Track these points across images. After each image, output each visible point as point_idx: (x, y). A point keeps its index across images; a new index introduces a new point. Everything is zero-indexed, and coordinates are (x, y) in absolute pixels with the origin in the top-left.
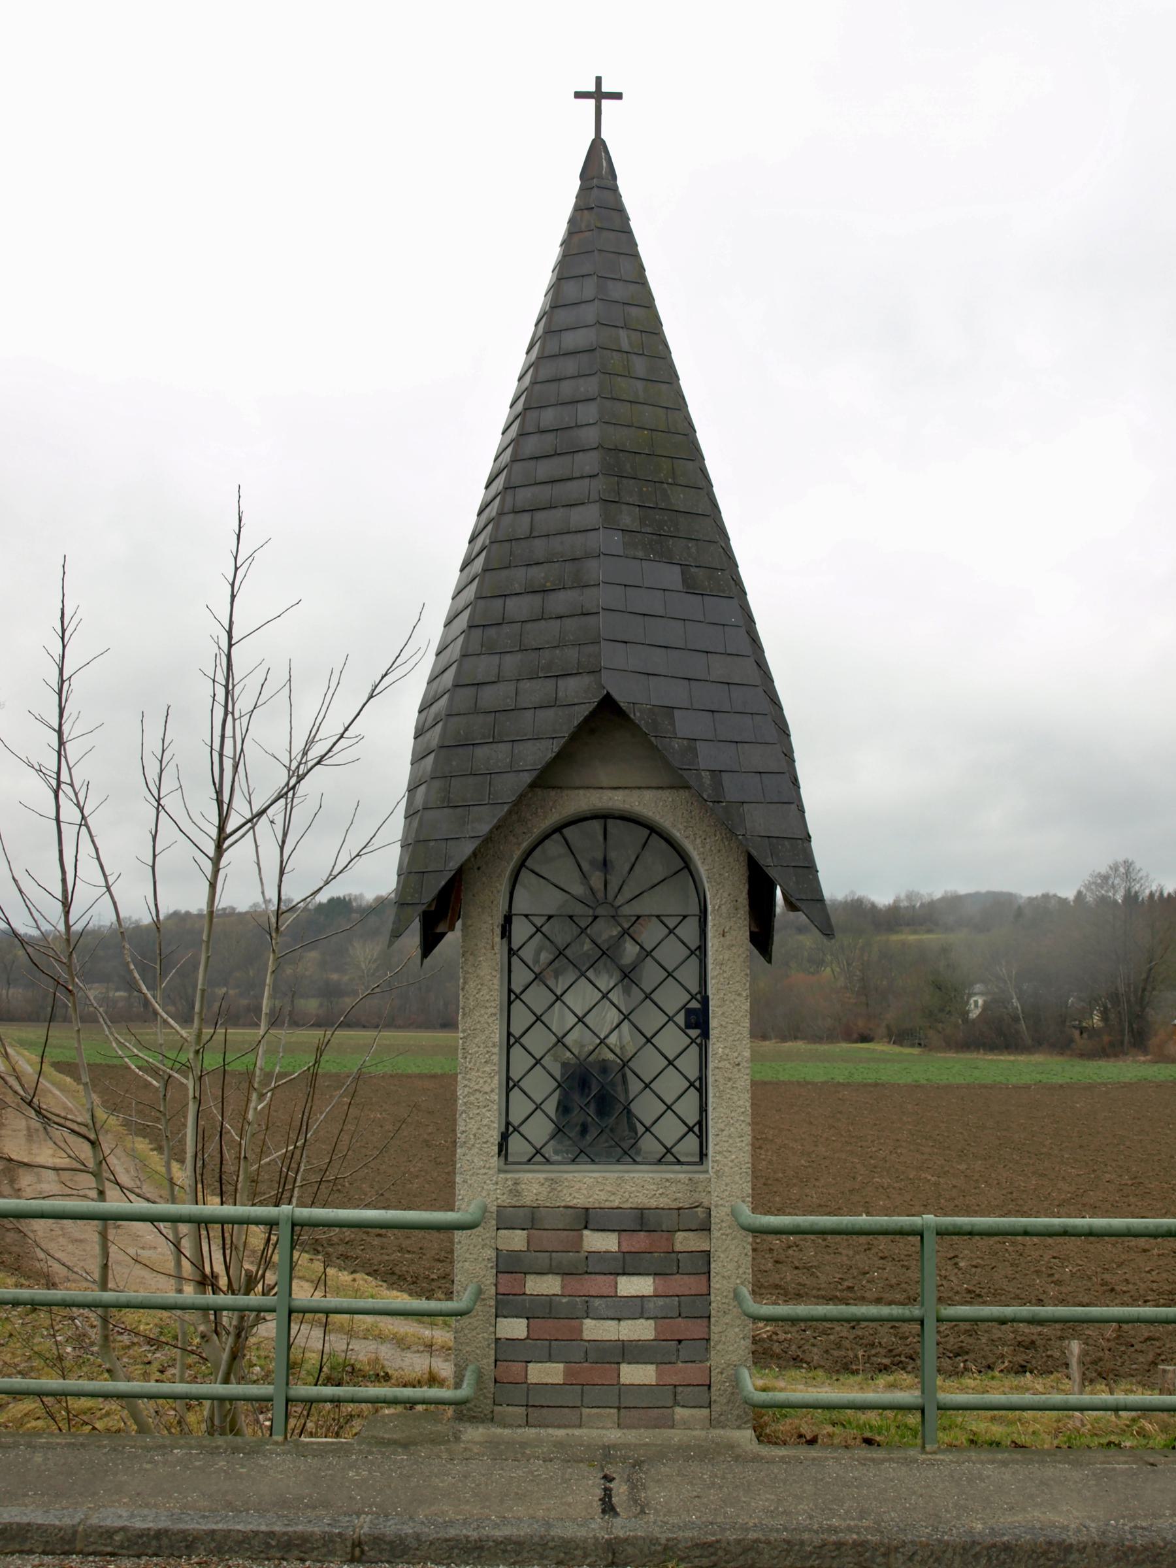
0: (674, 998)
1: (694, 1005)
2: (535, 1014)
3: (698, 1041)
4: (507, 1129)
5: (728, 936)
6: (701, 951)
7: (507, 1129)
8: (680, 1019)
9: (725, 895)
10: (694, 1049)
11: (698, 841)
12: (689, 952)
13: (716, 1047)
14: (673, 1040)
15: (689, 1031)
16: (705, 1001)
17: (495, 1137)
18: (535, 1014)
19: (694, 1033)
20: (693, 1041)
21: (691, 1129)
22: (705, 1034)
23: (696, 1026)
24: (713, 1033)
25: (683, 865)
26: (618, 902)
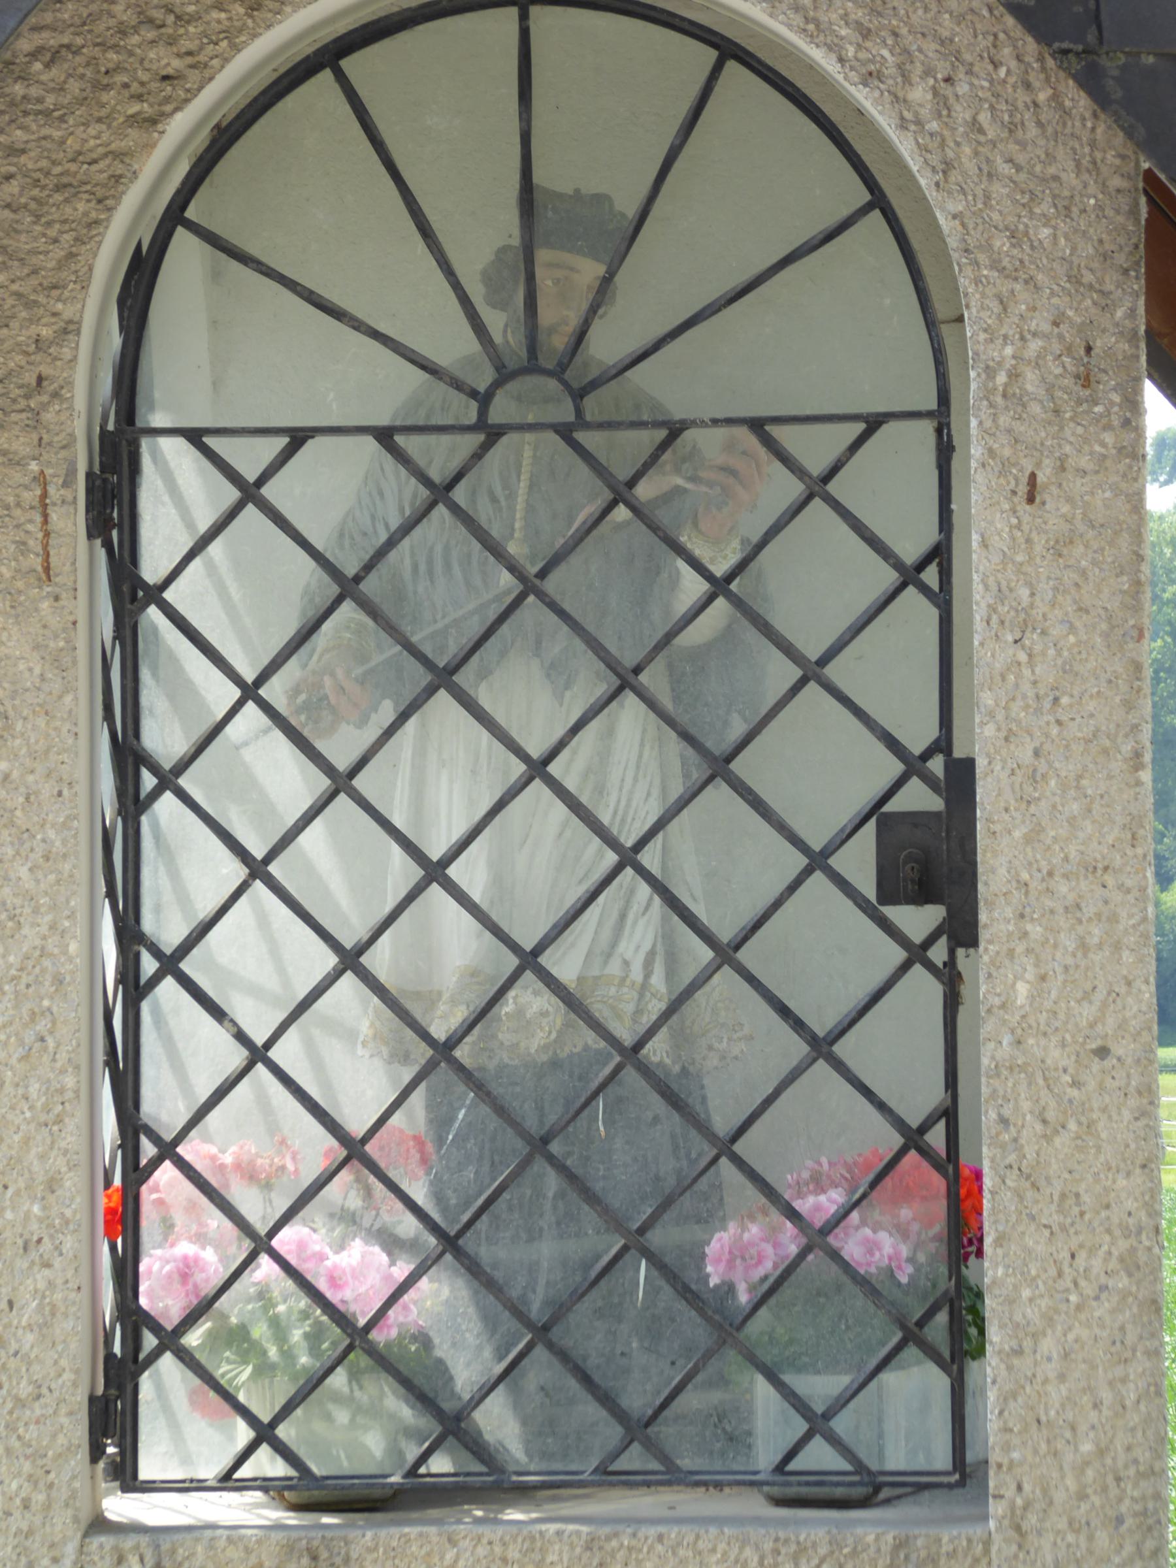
0: (828, 772)
1: (919, 798)
2: (839, 1066)
3: (938, 953)
4: (133, 1341)
5: (1054, 504)
6: (932, 572)
7: (133, 1341)
8: (859, 861)
9: (1040, 322)
10: (922, 988)
11: (919, 94)
12: (891, 577)
13: (1006, 974)
14: (834, 947)
15: (897, 914)
16: (960, 781)
17: (72, 1380)
18: (839, 1066)
19: (917, 920)
20: (917, 954)
21: (170, 964)
22: (962, 930)
23: (923, 894)
24: (994, 919)
25: (866, 197)
26: (607, 345)
